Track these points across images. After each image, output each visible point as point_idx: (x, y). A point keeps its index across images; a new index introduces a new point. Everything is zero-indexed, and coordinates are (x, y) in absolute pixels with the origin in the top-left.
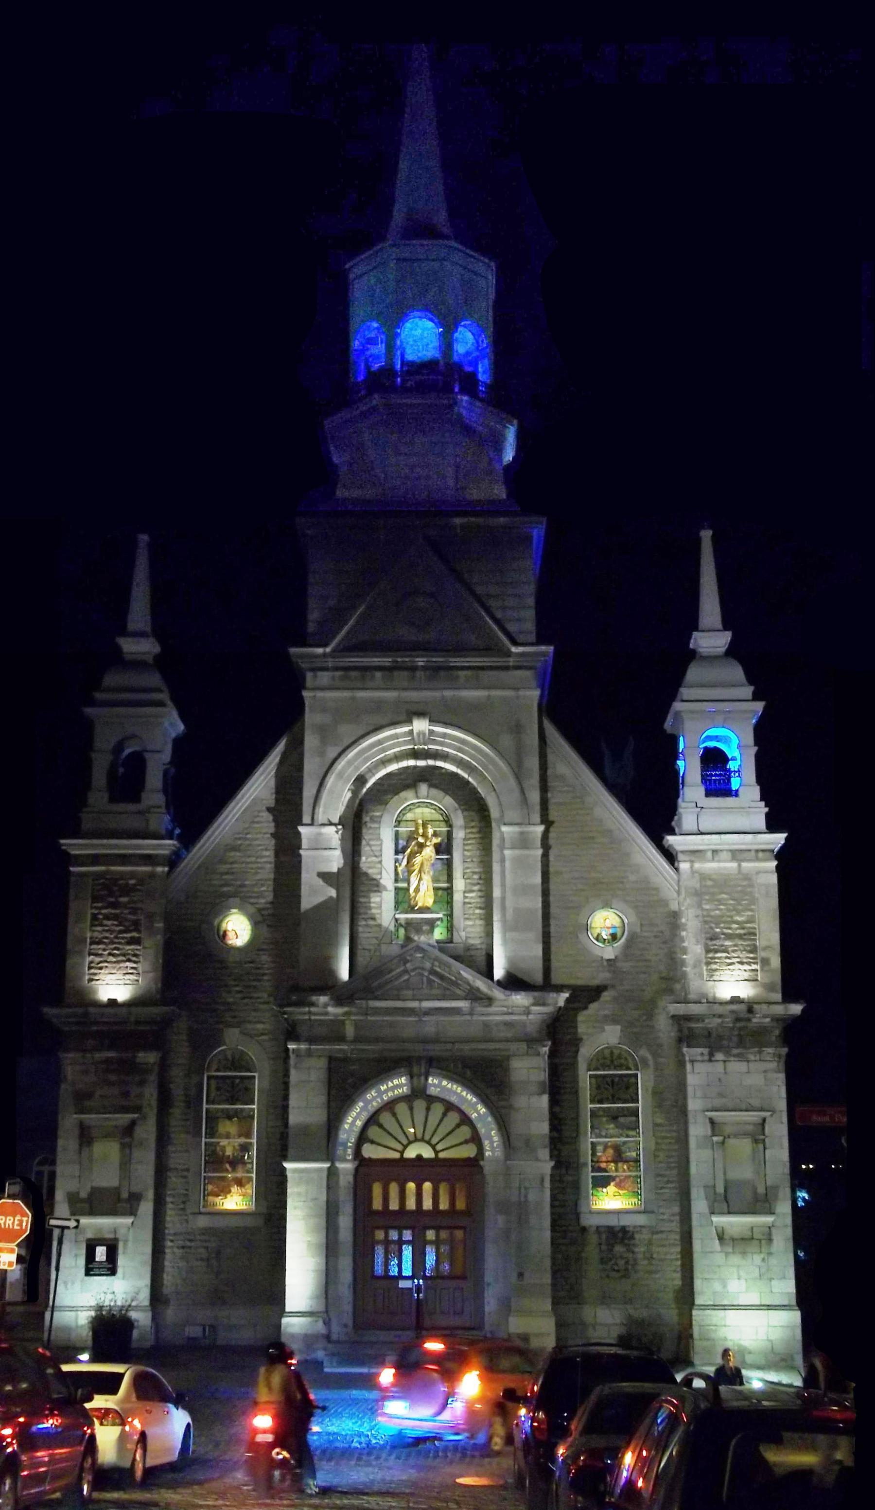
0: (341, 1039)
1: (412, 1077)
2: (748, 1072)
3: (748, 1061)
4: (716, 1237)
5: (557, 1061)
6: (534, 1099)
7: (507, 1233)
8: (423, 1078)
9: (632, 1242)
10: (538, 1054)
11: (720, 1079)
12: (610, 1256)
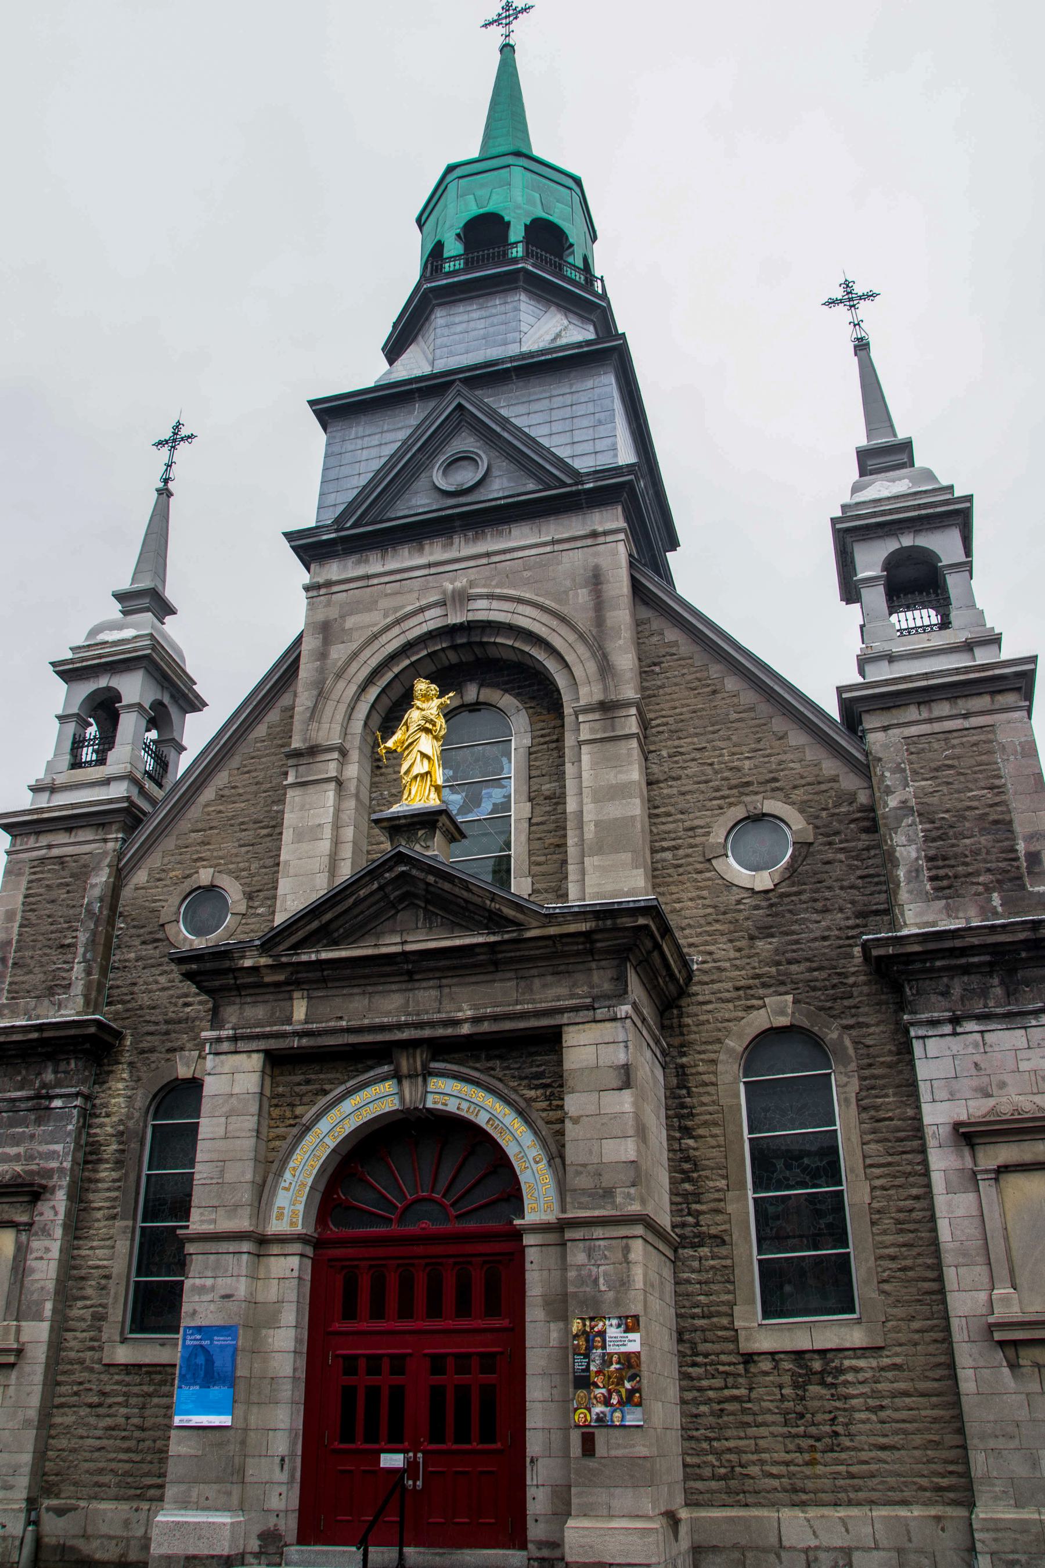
0: (289, 1021)
1: (400, 1082)
2: (1029, 1048)
3: (1025, 1028)
4: (1005, 1364)
5: (684, 1060)
6: (608, 1097)
7: (565, 1351)
8: (420, 1079)
9: (842, 1378)
10: (614, 1019)
11: (976, 1064)
12: (799, 1408)
